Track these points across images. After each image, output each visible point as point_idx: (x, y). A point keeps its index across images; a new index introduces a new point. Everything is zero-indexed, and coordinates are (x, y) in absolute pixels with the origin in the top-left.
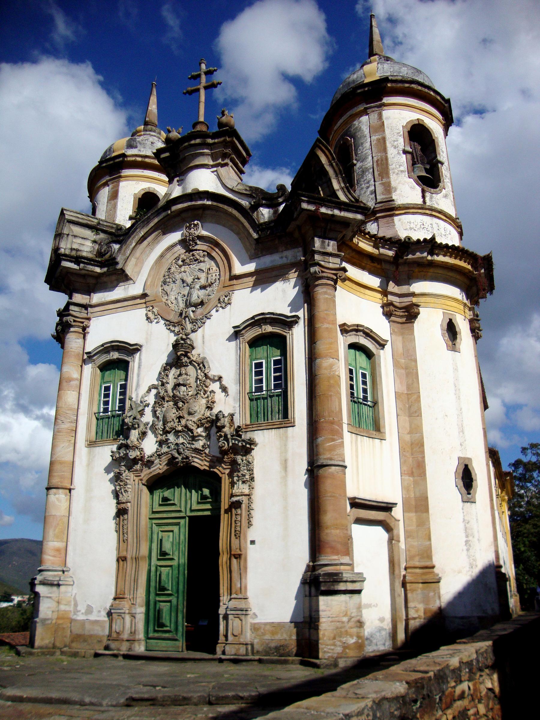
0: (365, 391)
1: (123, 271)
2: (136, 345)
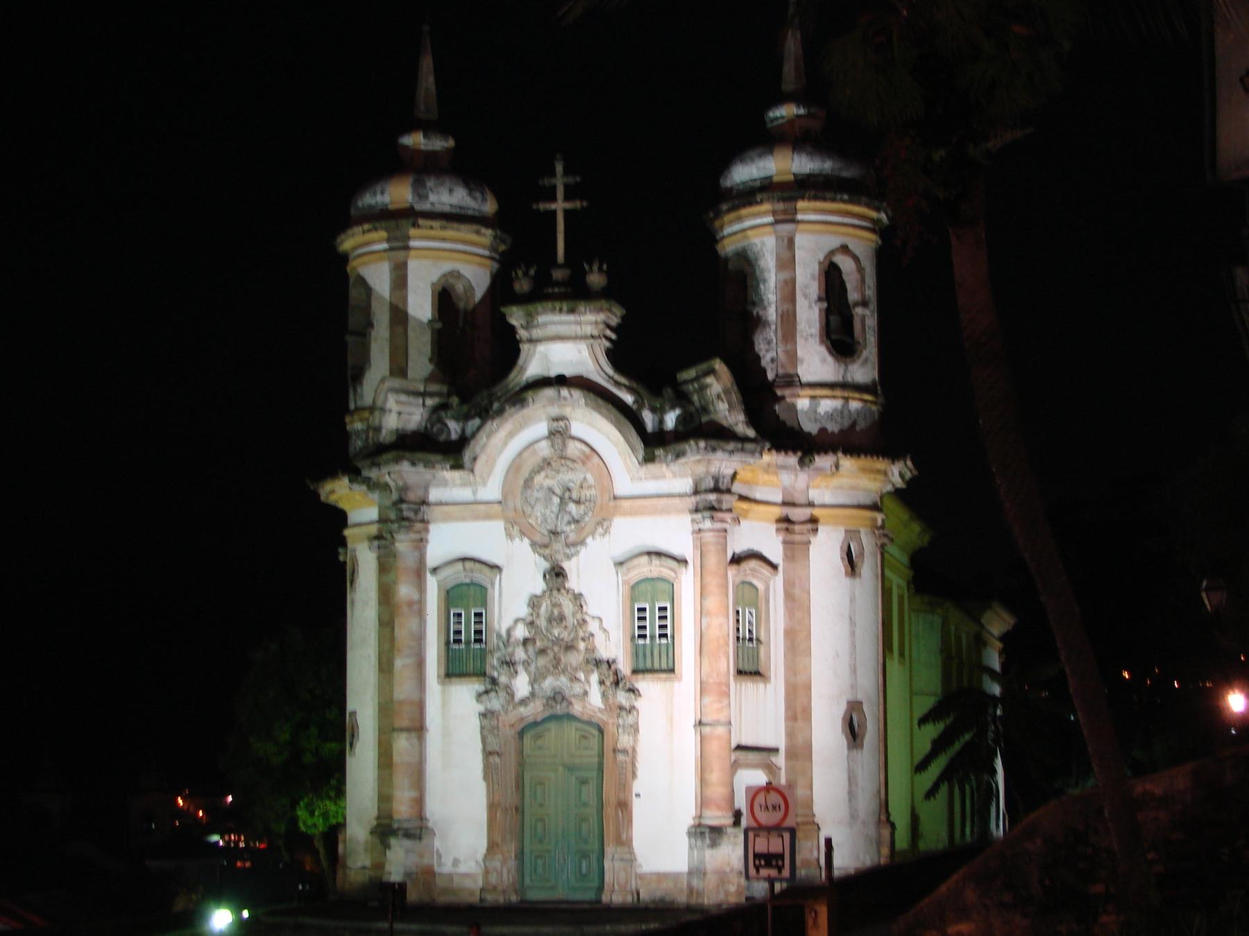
0: (750, 631)
1: (472, 471)
2: (495, 568)
